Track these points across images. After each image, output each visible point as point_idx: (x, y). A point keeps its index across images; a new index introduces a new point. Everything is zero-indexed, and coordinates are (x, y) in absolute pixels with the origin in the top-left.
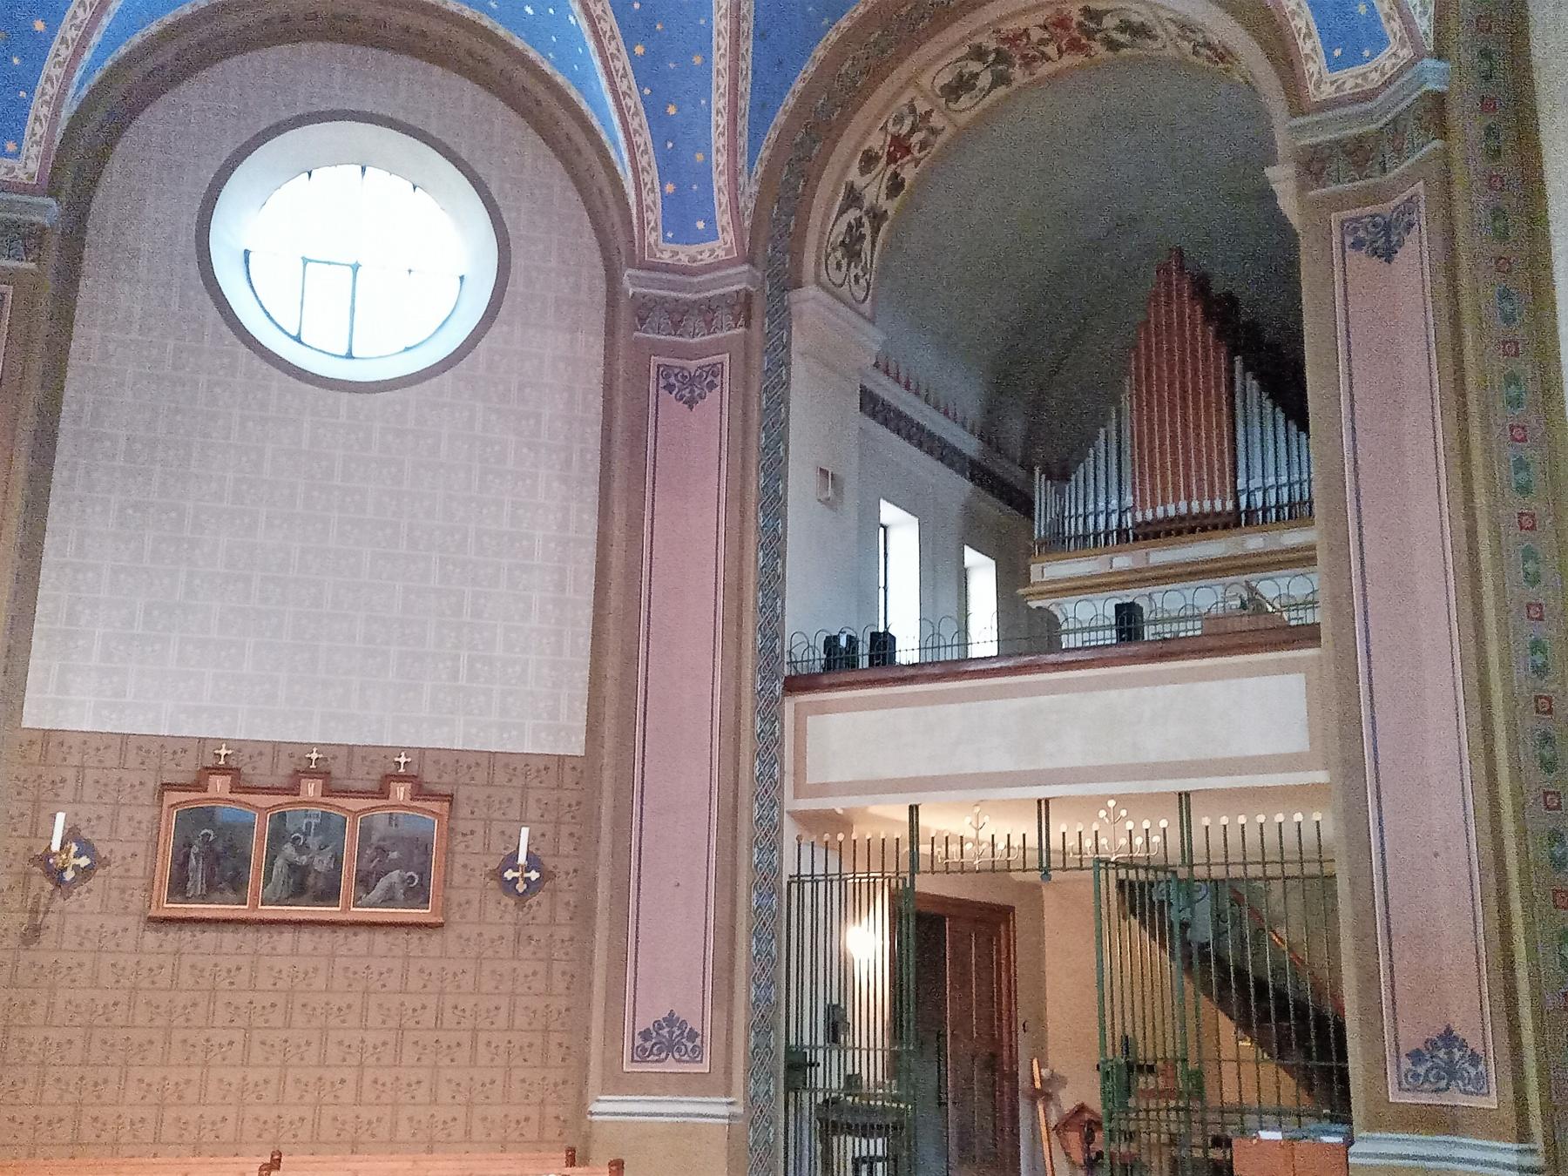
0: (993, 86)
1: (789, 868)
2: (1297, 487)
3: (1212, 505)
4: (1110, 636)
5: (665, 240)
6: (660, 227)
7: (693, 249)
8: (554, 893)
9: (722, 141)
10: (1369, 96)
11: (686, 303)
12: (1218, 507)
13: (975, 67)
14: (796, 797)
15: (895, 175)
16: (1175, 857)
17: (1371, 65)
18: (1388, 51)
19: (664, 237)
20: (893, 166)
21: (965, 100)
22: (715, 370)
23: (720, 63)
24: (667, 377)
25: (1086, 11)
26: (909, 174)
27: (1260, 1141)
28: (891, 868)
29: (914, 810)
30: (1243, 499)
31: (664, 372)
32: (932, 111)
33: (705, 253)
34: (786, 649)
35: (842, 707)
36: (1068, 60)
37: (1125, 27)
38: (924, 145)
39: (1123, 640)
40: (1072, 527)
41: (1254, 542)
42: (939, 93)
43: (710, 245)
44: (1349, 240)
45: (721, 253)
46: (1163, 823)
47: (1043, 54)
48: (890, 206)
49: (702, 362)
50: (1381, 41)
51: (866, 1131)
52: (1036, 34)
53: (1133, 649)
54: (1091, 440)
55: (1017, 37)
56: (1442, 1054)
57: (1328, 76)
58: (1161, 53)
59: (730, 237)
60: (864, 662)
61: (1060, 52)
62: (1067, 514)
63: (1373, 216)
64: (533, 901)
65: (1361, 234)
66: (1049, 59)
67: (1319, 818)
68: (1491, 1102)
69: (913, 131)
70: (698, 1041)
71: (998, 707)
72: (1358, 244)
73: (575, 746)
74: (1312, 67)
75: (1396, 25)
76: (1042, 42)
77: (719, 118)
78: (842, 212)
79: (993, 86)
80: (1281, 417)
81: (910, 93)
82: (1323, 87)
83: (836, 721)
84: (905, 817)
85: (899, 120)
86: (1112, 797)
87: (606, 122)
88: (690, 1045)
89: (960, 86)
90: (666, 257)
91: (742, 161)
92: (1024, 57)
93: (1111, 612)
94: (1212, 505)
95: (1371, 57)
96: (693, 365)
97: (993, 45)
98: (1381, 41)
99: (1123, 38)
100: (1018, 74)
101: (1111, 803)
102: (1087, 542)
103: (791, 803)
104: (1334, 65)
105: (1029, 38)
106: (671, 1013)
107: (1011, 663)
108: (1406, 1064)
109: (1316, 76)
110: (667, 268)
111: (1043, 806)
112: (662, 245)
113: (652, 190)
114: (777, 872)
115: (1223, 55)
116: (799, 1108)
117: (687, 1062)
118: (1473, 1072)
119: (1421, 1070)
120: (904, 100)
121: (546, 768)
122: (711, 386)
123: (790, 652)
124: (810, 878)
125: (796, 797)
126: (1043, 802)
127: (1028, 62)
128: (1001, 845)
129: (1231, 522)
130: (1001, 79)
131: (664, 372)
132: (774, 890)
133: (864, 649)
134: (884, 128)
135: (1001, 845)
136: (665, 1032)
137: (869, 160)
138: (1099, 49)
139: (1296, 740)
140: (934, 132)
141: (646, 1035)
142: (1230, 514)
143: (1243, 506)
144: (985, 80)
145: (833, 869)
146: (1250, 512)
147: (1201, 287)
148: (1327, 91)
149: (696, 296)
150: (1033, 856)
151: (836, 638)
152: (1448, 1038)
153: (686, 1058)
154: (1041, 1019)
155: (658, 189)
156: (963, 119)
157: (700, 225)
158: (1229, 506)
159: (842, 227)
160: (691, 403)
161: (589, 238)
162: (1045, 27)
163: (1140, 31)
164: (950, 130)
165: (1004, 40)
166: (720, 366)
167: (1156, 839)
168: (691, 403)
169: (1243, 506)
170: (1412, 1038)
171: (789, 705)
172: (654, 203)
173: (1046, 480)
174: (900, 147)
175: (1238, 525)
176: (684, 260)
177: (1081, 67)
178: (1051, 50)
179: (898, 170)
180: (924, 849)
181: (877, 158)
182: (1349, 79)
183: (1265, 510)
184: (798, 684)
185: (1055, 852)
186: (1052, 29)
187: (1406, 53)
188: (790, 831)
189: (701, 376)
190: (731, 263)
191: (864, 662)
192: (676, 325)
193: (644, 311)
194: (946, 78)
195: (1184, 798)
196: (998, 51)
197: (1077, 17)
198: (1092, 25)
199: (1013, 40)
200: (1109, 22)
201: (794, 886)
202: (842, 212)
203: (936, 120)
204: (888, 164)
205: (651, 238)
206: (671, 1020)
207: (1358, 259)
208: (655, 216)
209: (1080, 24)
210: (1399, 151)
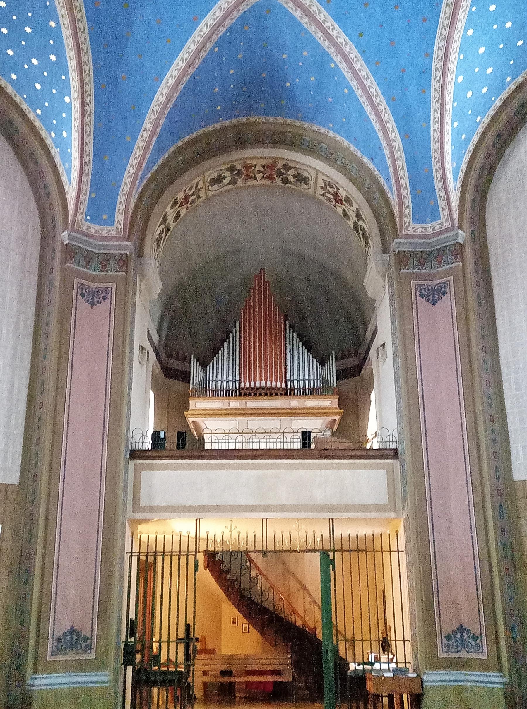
0: (229, 184)
7: (98, 228)
9: (129, 180)
10: (428, 237)
13: (227, 174)
15: (179, 212)
17: (431, 224)
35: (166, 468)
38: (193, 201)
39: (306, 447)
42: (209, 180)
43: (109, 227)
45: (114, 233)
48: (172, 225)
49: (99, 285)
52: (259, 168)
55: (251, 167)
57: (412, 225)
58: (307, 191)
59: (121, 226)
61: (263, 177)
66: (256, 178)
69: (193, 194)
71: (245, 473)
72: (422, 296)
74: (406, 220)
75: (446, 213)
76: (259, 172)
78: (160, 225)
79: (229, 184)
80: (306, 351)
81: (200, 178)
82: (409, 229)
83: (158, 475)
85: (190, 189)
89: (218, 180)
90: (84, 228)
92: (247, 175)
95: (431, 222)
96: (94, 286)
100: (240, 182)
102: (215, 393)
104: (415, 220)
110: (88, 235)
120: (196, 181)
122: (104, 298)
123: (132, 437)
124: (133, 554)
126: (264, 520)
127: (248, 177)
129: (285, 392)
131: (81, 286)
134: (185, 191)
137: (175, 203)
138: (278, 181)
140: (199, 197)
142: (283, 389)
144: (226, 181)
148: (410, 231)
149: (96, 251)
151: (159, 433)
156: (210, 194)
159: (158, 232)
160: (93, 304)
161: (33, 206)
162: (264, 167)
163: (302, 179)
166: (110, 289)
168: (93, 304)
172: (85, 200)
173: (197, 362)
182: (419, 229)
184: (135, 454)
185: (192, 537)
187: (447, 225)
190: (118, 239)
194: (215, 175)
196: (279, 175)
197: (280, 166)
198: (284, 171)
200: (292, 172)
202: (160, 225)
203: (202, 193)
204: (179, 207)
207: (422, 301)
210: (440, 262)
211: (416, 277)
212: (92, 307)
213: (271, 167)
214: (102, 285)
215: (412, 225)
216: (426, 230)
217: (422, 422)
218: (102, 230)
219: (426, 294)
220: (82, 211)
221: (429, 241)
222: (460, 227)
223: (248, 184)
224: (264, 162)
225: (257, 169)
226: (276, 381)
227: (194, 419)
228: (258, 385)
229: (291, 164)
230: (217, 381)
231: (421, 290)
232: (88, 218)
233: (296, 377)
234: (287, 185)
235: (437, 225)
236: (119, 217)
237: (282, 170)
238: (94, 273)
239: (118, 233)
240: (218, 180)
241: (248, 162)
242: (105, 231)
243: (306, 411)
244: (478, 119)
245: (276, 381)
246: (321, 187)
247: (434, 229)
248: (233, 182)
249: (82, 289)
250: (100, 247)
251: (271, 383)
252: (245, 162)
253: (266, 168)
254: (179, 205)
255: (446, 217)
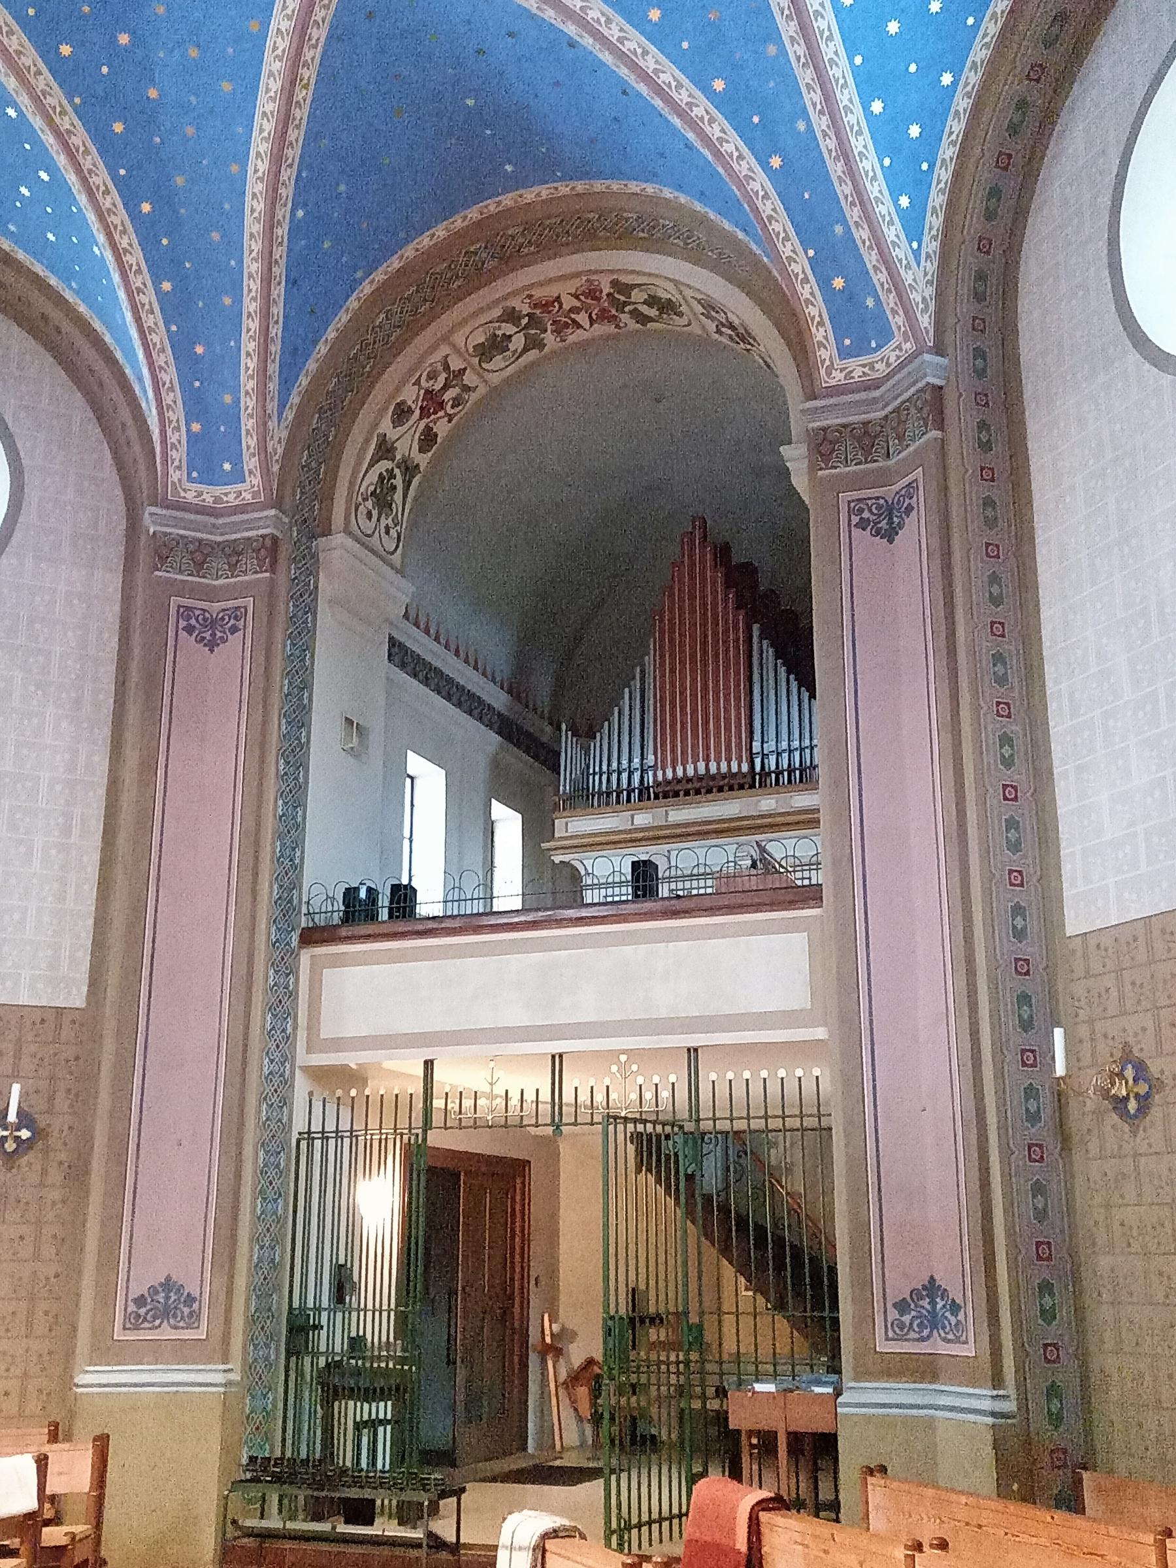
0: (526, 350)
1: (299, 1125)
2: (808, 751)
3: (729, 766)
4: (627, 892)
5: (190, 479)
6: (185, 467)
7: (218, 490)
8: (46, 1151)
9: (251, 384)
10: (876, 384)
11: (212, 545)
12: (735, 769)
13: (509, 329)
14: (309, 1051)
16: (683, 1112)
17: (878, 355)
18: (893, 344)
19: (189, 474)
20: (426, 420)
21: (498, 361)
22: (237, 613)
23: (251, 306)
24: (189, 618)
25: (615, 283)
26: (442, 428)
27: (754, 1393)
28: (403, 1124)
29: (429, 1065)
30: (758, 762)
31: (185, 612)
32: (465, 369)
33: (230, 494)
34: (305, 899)
36: (600, 329)
37: (652, 301)
38: (457, 402)
40: (595, 783)
41: (767, 803)
42: (471, 350)
43: (240, 487)
44: (855, 519)
46: (673, 1078)
47: (574, 321)
48: (422, 460)
49: (223, 605)
50: (885, 335)
51: (370, 1395)
52: (568, 302)
53: (648, 905)
54: (616, 701)
56: (925, 1303)
57: (838, 364)
59: (256, 480)
60: (384, 915)
61: (592, 322)
62: (591, 771)
63: (877, 498)
64: (24, 1161)
65: (866, 515)
66: (579, 326)
67: (818, 1074)
68: (968, 1351)
69: (446, 387)
70: (196, 1306)
72: (863, 525)
73: (77, 998)
74: (823, 354)
75: (900, 320)
77: (249, 361)
78: (371, 465)
79: (526, 350)
81: (444, 350)
82: (834, 373)
84: (420, 1071)
85: (432, 376)
86: (624, 1052)
87: (130, 353)
88: (186, 1310)
89: (494, 346)
90: (190, 496)
91: (272, 406)
93: (627, 869)
94: (729, 766)
95: (879, 347)
97: (526, 310)
98: (885, 335)
99: (653, 312)
100: (549, 338)
101: (623, 1058)
102: (611, 798)
103: (303, 1058)
104: (844, 353)
105: (561, 307)
106: (168, 1278)
107: (530, 917)
108: (893, 1314)
109: (827, 363)
111: (557, 1060)
112: (188, 485)
113: (178, 429)
114: (287, 1128)
115: (743, 336)
116: (300, 1373)
117: (183, 1328)
118: (953, 1321)
119: (906, 1319)
120: (438, 356)
121: (43, 1021)
122: (234, 630)
125: (309, 1051)
128: (514, 1101)
130: (534, 343)
131: (185, 612)
132: (284, 1147)
133: (384, 901)
134: (417, 382)
135: (514, 1101)
136: (161, 1297)
138: (625, 318)
139: (798, 998)
140: (467, 389)
141: (140, 1301)
143: (758, 768)
144: (518, 342)
145: (345, 1125)
146: (765, 774)
147: (723, 552)
148: (838, 377)
149: (219, 539)
150: (545, 1109)
151: (357, 889)
152: (932, 1288)
153: (182, 1324)
154: (553, 1272)
155: (183, 429)
156: (495, 379)
157: (227, 466)
158: (745, 768)
159: (373, 477)
162: (577, 297)
163: (667, 307)
164: (482, 390)
165: (536, 306)
167: (665, 1094)
169: (758, 768)
170: (899, 1288)
171: (306, 957)
174: (433, 402)
175: (752, 786)
176: (209, 500)
177: (609, 337)
178: (582, 318)
179: (431, 425)
180: (438, 1103)
181: (410, 411)
182: (857, 368)
183: (778, 773)
184: (313, 936)
185: (567, 1105)
186: (582, 298)
187: (908, 346)
188: (301, 1086)
189: (223, 619)
191: (384, 915)
192: (200, 565)
193: (164, 550)
195: (693, 1052)
197: (607, 289)
198: (622, 298)
199: (546, 306)
200: (637, 296)
201: (304, 1144)
202: (371, 465)
203: (469, 379)
204: (421, 418)
205: (175, 476)
206: (168, 1285)
208: (179, 455)
209: (609, 295)
210: (901, 438)
211: (856, 483)
212: (212, 651)
213: (593, 293)
214: (231, 604)
215: (838, 364)
216: (872, 368)
217: (855, 820)
218: (226, 494)
219: (873, 518)
220: (176, 463)
221: (876, 394)
222: (939, 350)
223: (571, 339)
224: (572, 286)
225: (566, 307)
226: (729, 761)
227: (566, 858)
228: (690, 772)
229: (625, 279)
230: (609, 774)
231: (861, 511)
232: (195, 474)
233: (796, 744)
234: (649, 325)
235: (891, 353)
236: (251, 463)
237: (617, 296)
238: (215, 583)
239: (255, 495)
240: (494, 346)
241: (538, 293)
242: (231, 497)
243: (779, 820)
244: (947, 79)
245: (729, 761)
246: (703, 314)
247: (888, 365)
248: (534, 343)
249: (189, 618)
250: (236, 528)
251: (739, 766)
252: (530, 296)
253: (582, 298)
254: (417, 412)
255: (903, 329)
